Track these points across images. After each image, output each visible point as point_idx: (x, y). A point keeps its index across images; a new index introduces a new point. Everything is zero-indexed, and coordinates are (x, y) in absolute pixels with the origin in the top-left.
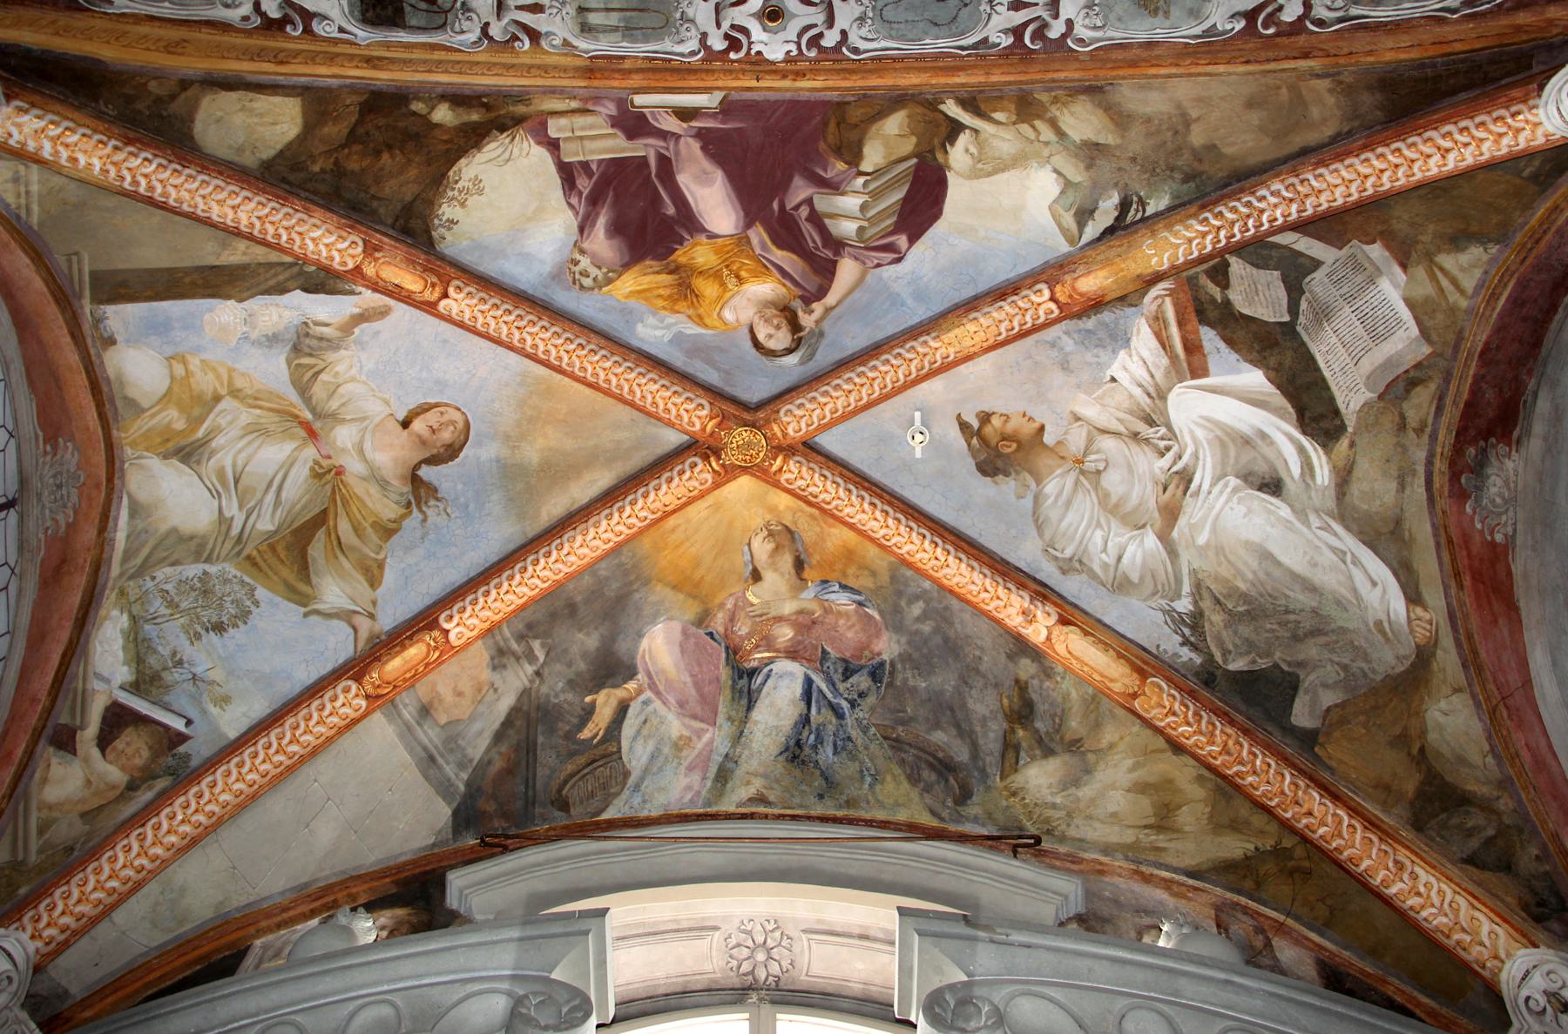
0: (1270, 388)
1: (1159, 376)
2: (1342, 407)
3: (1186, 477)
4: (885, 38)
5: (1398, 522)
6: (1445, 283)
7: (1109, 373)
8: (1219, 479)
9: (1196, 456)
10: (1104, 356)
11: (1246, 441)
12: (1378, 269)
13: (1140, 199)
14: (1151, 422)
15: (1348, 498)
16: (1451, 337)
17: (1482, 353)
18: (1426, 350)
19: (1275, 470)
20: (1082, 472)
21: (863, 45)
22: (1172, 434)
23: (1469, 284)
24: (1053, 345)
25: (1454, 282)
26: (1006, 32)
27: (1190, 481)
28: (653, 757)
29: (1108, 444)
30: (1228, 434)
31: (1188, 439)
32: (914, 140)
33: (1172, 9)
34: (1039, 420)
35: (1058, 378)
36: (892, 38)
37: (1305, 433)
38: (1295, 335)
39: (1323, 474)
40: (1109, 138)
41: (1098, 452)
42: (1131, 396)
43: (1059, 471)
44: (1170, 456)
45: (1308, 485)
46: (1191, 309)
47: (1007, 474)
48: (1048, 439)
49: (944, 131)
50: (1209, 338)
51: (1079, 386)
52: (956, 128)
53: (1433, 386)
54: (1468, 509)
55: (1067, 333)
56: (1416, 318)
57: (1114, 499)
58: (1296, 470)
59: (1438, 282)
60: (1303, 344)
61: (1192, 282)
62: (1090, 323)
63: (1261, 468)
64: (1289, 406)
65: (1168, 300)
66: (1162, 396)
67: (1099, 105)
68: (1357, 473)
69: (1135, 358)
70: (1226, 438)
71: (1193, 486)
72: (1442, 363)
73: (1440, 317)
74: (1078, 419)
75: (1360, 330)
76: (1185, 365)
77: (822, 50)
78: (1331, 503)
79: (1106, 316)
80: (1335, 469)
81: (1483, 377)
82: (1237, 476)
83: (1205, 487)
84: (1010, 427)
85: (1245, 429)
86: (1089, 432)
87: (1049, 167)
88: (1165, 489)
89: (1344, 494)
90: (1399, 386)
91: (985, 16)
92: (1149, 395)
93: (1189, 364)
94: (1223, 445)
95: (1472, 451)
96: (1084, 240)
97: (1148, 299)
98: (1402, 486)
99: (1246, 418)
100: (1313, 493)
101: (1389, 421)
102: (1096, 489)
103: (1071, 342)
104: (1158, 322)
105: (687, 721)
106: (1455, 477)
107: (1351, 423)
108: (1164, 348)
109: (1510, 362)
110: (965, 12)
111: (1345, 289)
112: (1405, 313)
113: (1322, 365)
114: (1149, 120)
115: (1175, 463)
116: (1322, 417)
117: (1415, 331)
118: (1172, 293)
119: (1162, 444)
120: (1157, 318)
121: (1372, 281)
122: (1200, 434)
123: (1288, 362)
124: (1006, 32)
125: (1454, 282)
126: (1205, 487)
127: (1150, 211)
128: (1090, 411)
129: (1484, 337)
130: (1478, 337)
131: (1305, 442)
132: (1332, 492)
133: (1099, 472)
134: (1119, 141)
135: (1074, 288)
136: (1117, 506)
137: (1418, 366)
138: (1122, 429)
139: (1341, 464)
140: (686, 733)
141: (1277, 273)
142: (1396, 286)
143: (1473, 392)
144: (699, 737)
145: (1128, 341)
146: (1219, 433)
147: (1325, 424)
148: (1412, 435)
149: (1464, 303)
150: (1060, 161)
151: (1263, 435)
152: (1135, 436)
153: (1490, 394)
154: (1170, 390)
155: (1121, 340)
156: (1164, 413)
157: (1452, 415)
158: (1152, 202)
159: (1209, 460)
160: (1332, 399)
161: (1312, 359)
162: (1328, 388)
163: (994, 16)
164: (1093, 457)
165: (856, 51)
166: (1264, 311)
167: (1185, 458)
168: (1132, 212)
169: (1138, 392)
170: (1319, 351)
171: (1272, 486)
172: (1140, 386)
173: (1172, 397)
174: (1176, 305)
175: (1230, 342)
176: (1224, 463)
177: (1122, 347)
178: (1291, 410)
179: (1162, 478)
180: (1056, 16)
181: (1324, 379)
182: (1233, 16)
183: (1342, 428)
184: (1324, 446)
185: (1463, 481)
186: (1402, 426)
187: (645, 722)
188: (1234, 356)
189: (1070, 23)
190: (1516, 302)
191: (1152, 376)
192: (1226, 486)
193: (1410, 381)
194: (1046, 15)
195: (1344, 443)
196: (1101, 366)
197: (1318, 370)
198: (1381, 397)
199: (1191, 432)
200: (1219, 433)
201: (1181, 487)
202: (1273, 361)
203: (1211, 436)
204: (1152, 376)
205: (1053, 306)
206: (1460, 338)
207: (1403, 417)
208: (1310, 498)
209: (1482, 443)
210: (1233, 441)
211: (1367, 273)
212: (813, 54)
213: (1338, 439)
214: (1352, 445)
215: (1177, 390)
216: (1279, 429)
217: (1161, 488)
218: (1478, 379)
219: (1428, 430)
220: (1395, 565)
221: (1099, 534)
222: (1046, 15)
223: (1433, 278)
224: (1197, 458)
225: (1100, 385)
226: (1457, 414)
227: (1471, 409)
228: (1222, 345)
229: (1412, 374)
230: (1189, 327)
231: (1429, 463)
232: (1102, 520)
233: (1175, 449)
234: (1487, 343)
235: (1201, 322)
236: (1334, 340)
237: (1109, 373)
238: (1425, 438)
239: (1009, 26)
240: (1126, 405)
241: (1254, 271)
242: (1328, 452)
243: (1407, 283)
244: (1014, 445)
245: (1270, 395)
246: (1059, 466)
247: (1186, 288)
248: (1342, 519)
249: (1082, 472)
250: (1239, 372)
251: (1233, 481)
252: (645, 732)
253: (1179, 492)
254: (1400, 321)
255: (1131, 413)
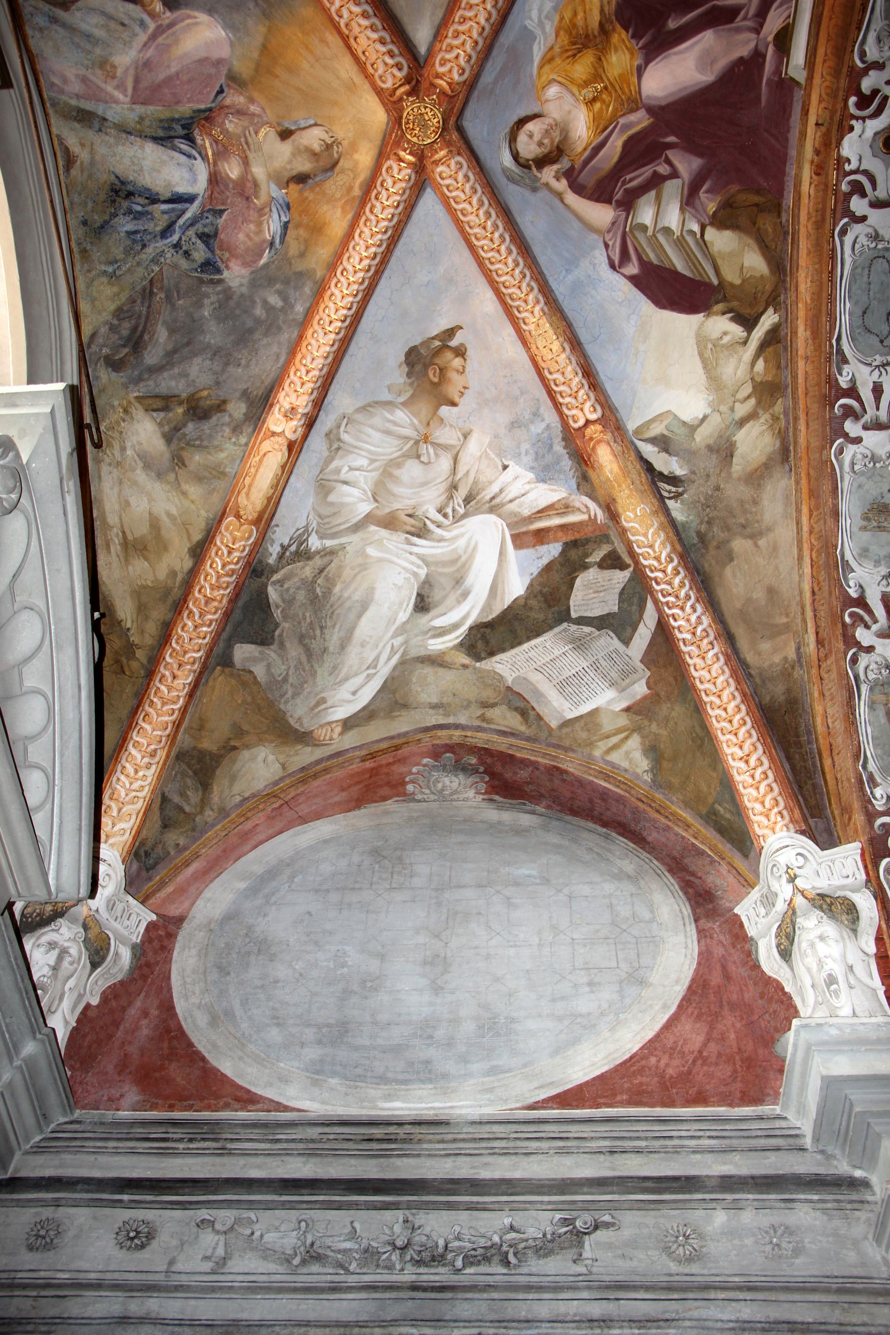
0: (508, 602)
1: (512, 507)
2: (497, 658)
3: (421, 532)
4: (854, 261)
5: (405, 706)
6: (615, 740)
7: (511, 463)
8: (423, 560)
9: (441, 540)
10: (527, 459)
11: (458, 581)
12: (623, 690)
13: (681, 494)
14: (467, 500)
15: (420, 665)
16: (567, 743)
17: (557, 768)
18: (554, 724)
19: (436, 606)
20: (417, 442)
21: (848, 239)
22: (458, 519)
23: (615, 757)
24: (536, 414)
25: (615, 747)
26: (853, 381)
27: (419, 536)
28: (88, 36)
29: (445, 463)
30: (464, 565)
31: (455, 532)
32: (738, 282)
33: (868, 534)
34: (461, 401)
35: (503, 418)
36: (854, 268)
37: (471, 628)
38: (559, 621)
39: (437, 645)
40: (738, 467)
41: (436, 455)
42: (490, 483)
43: (415, 421)
44: (439, 518)
45: (426, 633)
46: (577, 536)
47: (409, 375)
48: (444, 410)
49: (746, 311)
50: (552, 550)
51: (496, 436)
52: (748, 322)
53: (523, 728)
54: (426, 761)
55: (548, 427)
56: (581, 717)
57: (396, 472)
58: (438, 622)
59: (615, 734)
60: (551, 628)
61: (605, 538)
62: (559, 447)
63: (436, 595)
64: (494, 616)
65: (585, 517)
66: (494, 508)
67: (770, 458)
68: (441, 671)
69: (527, 487)
70: (460, 563)
71: (415, 540)
72: (543, 735)
73: (584, 735)
74: (465, 436)
75: (567, 673)
76: (524, 529)
77: (848, 196)
78: (414, 653)
79: (567, 463)
80: (443, 653)
81: (538, 769)
82: (427, 575)
83: (415, 549)
84: (453, 375)
85: (469, 581)
86: (453, 446)
87: (708, 411)
88: (410, 516)
89: (422, 662)
90: (521, 705)
91: (870, 360)
92: (493, 498)
93: (525, 533)
94: (454, 562)
95: (474, 761)
96: (641, 445)
97: (586, 500)
98: (434, 707)
99: (480, 580)
100: (420, 638)
101: (488, 694)
102: (403, 456)
103: (539, 431)
104: (565, 508)
105: (132, 72)
106: (450, 748)
107: (487, 665)
108: (539, 512)
109: (553, 790)
110: (875, 341)
111: (604, 663)
112: (585, 709)
113: (533, 642)
114: (755, 502)
115: (433, 522)
116: (487, 642)
117: (570, 715)
118: (592, 521)
119: (449, 511)
120: (567, 507)
121: (612, 685)
122: (461, 543)
123: (533, 615)
124: (853, 381)
125: (615, 747)
126: (415, 549)
127: (670, 504)
128: (473, 447)
129: (571, 770)
130: (571, 765)
131: (463, 629)
132: (423, 653)
133: (418, 457)
134: (735, 475)
135: (599, 441)
136: (391, 475)
137: (539, 718)
138: (459, 475)
139: (447, 658)
140: (119, 72)
141: (615, 609)
142: (610, 702)
143: (523, 761)
144: (117, 87)
145: (544, 481)
146: (463, 559)
147: (480, 645)
148: (479, 713)
149: (597, 753)
150: (716, 420)
151: (465, 595)
152: (454, 487)
153: (523, 774)
154: (500, 516)
155: (545, 473)
156: (478, 511)
157: (501, 744)
158: (678, 505)
159: (439, 551)
160: (503, 650)
161: (538, 635)
162: (512, 647)
163: (869, 369)
164: (431, 450)
165: (843, 232)
166: (580, 597)
167: (438, 531)
168: (668, 487)
169: (495, 489)
170: (546, 640)
171: (422, 605)
172: (501, 491)
173: (492, 518)
174: (581, 523)
175: (548, 568)
176: (437, 563)
177: (537, 475)
178: (490, 618)
179: (419, 513)
180: (865, 428)
181: (520, 643)
182: (861, 586)
183: (479, 659)
184: (461, 644)
185: (448, 755)
186: (485, 705)
187: (123, 25)
188: (535, 571)
189: (858, 440)
190: (605, 795)
191: (511, 501)
192: (418, 567)
193: (525, 710)
194: (867, 418)
195: (466, 660)
196: (517, 456)
197: (529, 639)
198: (509, 689)
199: (462, 535)
200: (463, 559)
201: (413, 529)
202: (533, 602)
203: (461, 552)
204: (511, 501)
205: (581, 422)
206: (567, 749)
207: (493, 705)
208: (416, 635)
209: (482, 769)
210: (458, 570)
211: (619, 681)
212: (844, 187)
213: (469, 655)
214: (465, 666)
215: (500, 521)
216: (473, 607)
217: (410, 512)
218: (534, 765)
219: (484, 725)
220: (372, 707)
221: (364, 462)
222: (867, 418)
223: (618, 731)
224: (440, 541)
225: (499, 455)
226: (503, 748)
227: (508, 759)
228: (545, 561)
229: (532, 713)
230: (560, 534)
231: (457, 726)
232: (377, 464)
233: (446, 522)
234: (566, 772)
235: (566, 544)
236: (557, 653)
237: (511, 463)
238: (477, 723)
239: (858, 384)
240: (482, 479)
241: (618, 591)
242: (455, 647)
243: (613, 711)
244: (436, 380)
245: (502, 600)
246: (420, 422)
247: (598, 533)
248: (402, 663)
249: (417, 442)
250: (521, 574)
251: (423, 572)
252: (113, 25)
253: (409, 528)
254: (577, 704)
255: (475, 483)
